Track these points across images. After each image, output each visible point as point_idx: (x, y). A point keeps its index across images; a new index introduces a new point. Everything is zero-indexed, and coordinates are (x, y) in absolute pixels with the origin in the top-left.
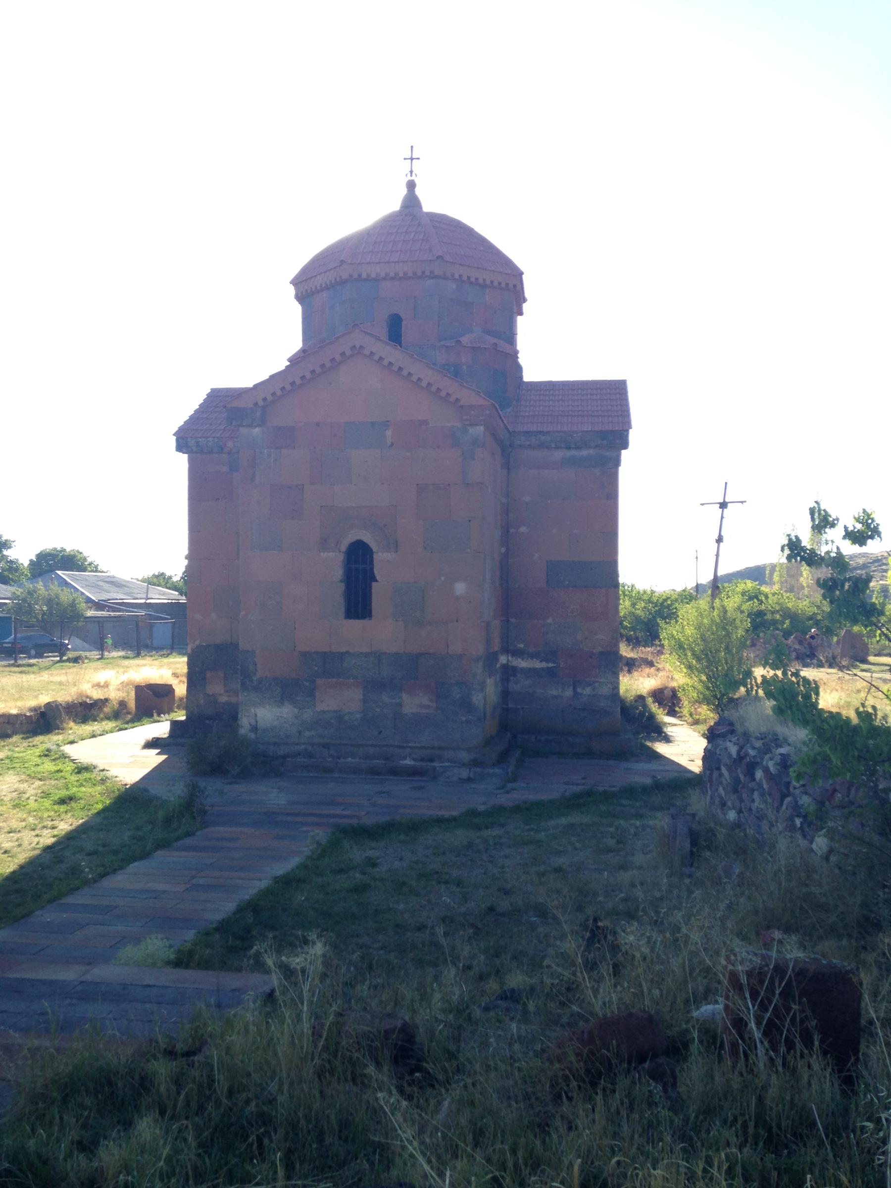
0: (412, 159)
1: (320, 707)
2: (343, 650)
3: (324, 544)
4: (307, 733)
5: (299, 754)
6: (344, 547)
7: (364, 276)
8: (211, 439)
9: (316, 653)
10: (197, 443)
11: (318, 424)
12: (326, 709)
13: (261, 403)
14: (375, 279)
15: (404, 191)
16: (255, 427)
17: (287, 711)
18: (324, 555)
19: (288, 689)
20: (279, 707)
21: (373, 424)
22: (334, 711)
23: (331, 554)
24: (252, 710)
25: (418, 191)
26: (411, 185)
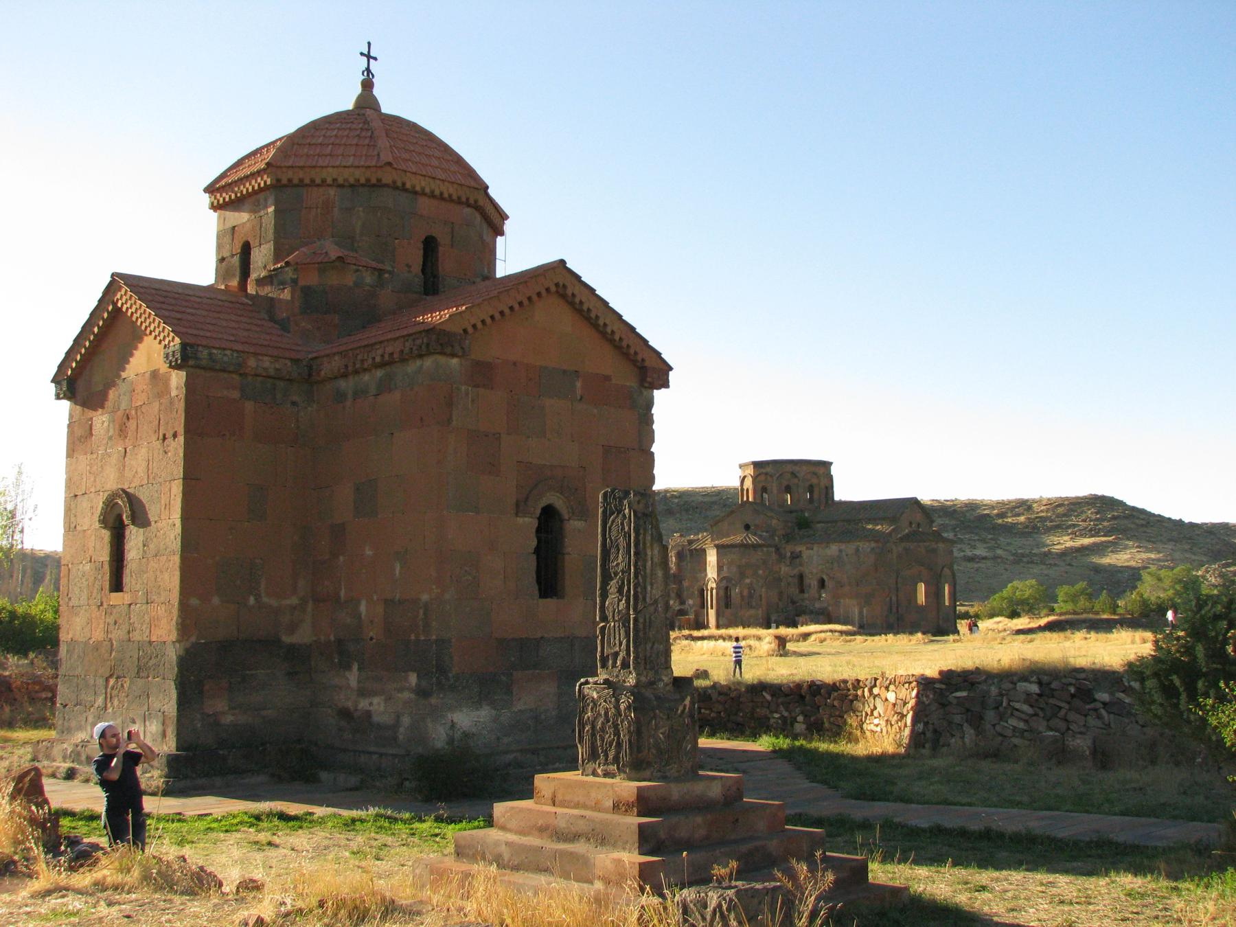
0: (369, 57)
1: (519, 706)
2: (539, 635)
3: (520, 508)
4: (506, 740)
5: (509, 765)
6: (538, 512)
7: (408, 186)
8: (228, 352)
9: (513, 639)
10: (210, 354)
11: (515, 364)
12: (523, 708)
13: (470, 330)
14: (416, 193)
15: (359, 90)
16: (453, 355)
17: (484, 714)
18: (520, 520)
19: (488, 687)
20: (477, 709)
21: (565, 371)
22: (531, 710)
23: (526, 519)
24: (449, 715)
25: (376, 92)
26: (368, 85)
